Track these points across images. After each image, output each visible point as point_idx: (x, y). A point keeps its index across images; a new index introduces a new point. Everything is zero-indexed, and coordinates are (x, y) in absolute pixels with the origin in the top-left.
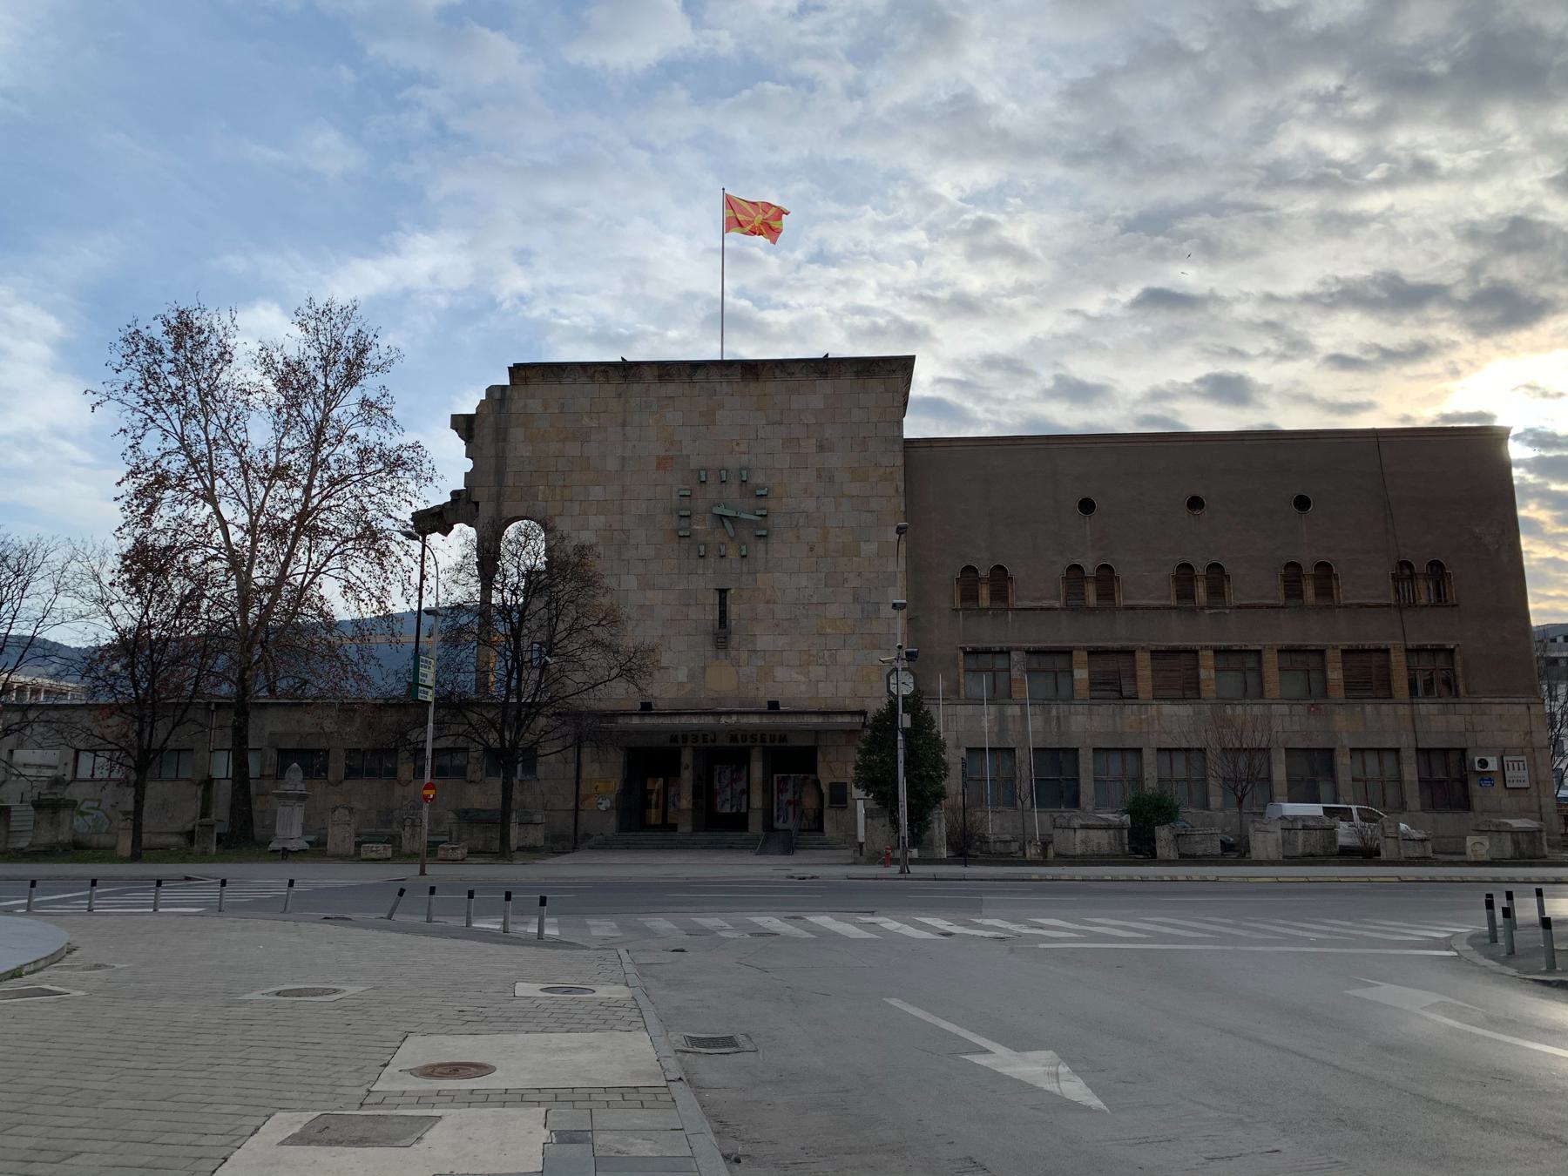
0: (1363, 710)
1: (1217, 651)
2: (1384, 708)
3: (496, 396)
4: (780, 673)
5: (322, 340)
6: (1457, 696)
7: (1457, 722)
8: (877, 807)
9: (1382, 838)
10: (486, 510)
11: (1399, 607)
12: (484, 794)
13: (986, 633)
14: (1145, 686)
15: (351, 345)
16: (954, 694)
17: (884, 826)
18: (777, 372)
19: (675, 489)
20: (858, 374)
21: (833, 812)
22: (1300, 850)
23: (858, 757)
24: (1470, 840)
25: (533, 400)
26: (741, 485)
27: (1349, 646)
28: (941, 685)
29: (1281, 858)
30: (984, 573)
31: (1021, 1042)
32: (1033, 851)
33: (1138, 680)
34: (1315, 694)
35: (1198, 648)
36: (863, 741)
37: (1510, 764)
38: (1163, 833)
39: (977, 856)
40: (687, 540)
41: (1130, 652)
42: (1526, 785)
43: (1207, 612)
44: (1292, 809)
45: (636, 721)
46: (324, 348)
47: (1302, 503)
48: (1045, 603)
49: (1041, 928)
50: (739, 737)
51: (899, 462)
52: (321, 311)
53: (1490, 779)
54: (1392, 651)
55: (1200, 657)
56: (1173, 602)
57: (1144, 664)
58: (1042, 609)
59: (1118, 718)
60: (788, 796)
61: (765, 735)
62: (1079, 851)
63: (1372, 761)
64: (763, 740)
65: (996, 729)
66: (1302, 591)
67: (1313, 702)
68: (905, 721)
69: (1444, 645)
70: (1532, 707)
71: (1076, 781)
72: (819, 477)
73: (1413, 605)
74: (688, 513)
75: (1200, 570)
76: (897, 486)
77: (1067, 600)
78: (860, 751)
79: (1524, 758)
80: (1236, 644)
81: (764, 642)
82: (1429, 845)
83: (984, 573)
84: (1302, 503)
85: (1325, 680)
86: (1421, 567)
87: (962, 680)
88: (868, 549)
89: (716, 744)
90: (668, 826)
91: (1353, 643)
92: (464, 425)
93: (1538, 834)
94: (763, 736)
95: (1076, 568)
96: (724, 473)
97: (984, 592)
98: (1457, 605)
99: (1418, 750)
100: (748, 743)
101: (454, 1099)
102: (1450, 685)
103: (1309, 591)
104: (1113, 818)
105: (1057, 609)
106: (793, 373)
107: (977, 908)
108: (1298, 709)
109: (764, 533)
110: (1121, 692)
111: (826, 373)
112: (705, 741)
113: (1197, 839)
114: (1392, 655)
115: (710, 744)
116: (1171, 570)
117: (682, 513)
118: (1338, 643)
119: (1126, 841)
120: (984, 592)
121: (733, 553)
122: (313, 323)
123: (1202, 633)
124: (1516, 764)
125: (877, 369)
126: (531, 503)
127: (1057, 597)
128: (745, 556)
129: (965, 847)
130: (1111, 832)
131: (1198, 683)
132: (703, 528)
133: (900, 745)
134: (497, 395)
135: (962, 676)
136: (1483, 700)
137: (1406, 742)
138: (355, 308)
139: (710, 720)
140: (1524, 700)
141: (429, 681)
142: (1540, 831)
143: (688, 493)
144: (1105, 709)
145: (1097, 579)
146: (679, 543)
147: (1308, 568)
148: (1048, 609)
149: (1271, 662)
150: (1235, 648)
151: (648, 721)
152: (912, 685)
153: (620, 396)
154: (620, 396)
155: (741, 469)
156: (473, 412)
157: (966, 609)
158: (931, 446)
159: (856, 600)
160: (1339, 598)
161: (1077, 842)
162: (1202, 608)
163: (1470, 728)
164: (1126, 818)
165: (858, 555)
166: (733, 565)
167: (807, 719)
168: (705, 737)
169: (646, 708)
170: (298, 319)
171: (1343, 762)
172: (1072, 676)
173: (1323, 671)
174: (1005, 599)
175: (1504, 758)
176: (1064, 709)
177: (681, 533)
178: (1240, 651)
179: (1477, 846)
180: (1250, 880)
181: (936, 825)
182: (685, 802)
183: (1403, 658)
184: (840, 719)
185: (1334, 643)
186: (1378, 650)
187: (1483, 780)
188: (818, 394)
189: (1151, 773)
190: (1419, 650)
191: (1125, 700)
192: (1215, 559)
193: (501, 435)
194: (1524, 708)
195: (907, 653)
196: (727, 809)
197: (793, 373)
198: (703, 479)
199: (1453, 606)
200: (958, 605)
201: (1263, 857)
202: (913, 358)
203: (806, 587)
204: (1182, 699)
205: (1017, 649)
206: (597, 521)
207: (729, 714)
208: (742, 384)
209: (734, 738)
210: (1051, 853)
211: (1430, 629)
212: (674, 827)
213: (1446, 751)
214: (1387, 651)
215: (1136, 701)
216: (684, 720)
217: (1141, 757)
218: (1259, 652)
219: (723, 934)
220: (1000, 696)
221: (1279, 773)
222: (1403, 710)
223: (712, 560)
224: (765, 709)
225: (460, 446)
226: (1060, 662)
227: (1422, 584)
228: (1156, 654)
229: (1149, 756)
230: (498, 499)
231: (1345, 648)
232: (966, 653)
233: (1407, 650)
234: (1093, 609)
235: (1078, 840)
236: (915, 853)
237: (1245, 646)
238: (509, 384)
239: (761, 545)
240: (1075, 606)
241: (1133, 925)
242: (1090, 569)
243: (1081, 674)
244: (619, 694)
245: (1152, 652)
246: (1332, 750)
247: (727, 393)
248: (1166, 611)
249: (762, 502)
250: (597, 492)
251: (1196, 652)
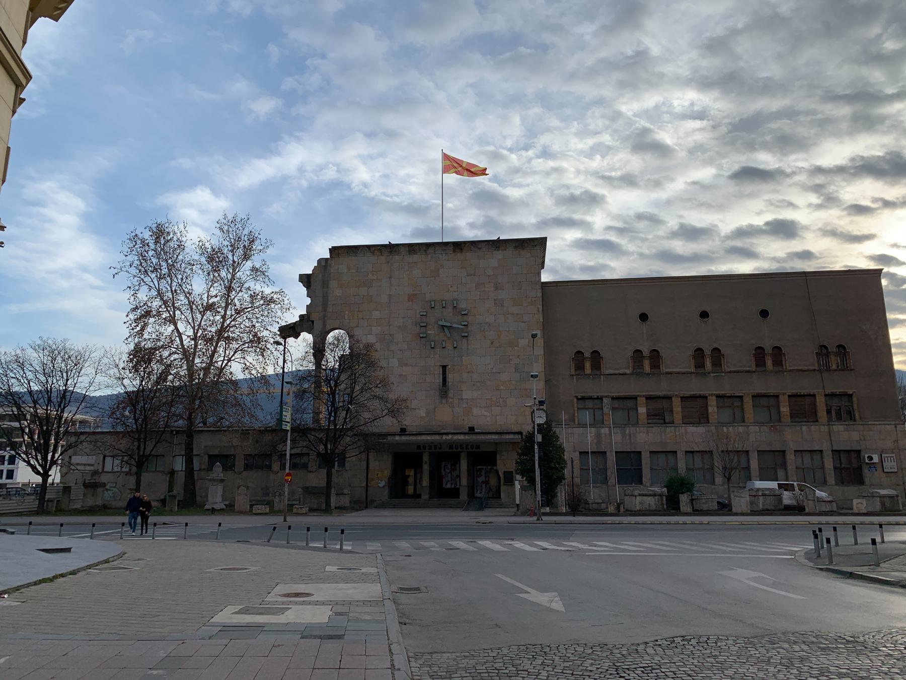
0: (801, 429)
1: (718, 397)
2: (814, 428)
3: (323, 264)
4: (476, 411)
5: (231, 237)
6: (855, 420)
7: (855, 435)
8: (528, 485)
9: (806, 501)
10: (318, 325)
11: (820, 371)
12: (317, 478)
13: (589, 388)
14: (678, 417)
15: (246, 239)
16: (572, 421)
17: (531, 495)
18: (472, 247)
19: (418, 311)
20: (516, 247)
21: (505, 487)
22: (761, 507)
23: (516, 457)
24: (855, 501)
25: (343, 265)
26: (453, 309)
28: (564, 417)
29: (749, 512)
30: (587, 355)
31: (543, 589)
32: (612, 508)
33: (674, 412)
34: (774, 420)
35: (707, 395)
36: (520, 448)
37: (886, 459)
38: (684, 498)
39: (582, 511)
40: (425, 339)
41: (669, 398)
42: (896, 470)
43: (712, 375)
44: (759, 484)
45: (397, 438)
46: (232, 240)
47: (764, 314)
48: (621, 371)
49: (595, 546)
50: (454, 446)
51: (540, 295)
52: (230, 221)
53: (875, 467)
54: (817, 396)
56: (693, 370)
57: (677, 404)
58: (620, 374)
59: (663, 434)
60: (481, 479)
61: (468, 445)
62: (638, 508)
63: (807, 458)
64: (467, 448)
65: (595, 441)
66: (765, 363)
67: (772, 424)
68: (539, 438)
69: (847, 392)
70: (898, 426)
71: (640, 470)
73: (828, 369)
74: (425, 324)
75: (707, 352)
77: (634, 368)
78: (518, 454)
79: (894, 455)
80: (728, 392)
81: (467, 395)
82: (834, 504)
83: (587, 355)
84: (764, 314)
85: (779, 412)
86: (832, 348)
87: (576, 414)
89: (441, 450)
90: (416, 496)
91: (795, 391)
92: (306, 280)
93: (896, 498)
94: (467, 446)
95: (638, 352)
96: (444, 302)
97: (588, 365)
98: (854, 370)
99: (832, 451)
100: (459, 450)
101: (296, 603)
102: (851, 416)
103: (769, 363)
104: (657, 489)
105: (628, 374)
106: (481, 248)
107: (568, 537)
108: (764, 428)
109: (466, 334)
110: (664, 420)
111: (499, 247)
112: (435, 449)
113: (704, 501)
114: (817, 398)
115: (438, 450)
116: (691, 352)
117: (422, 325)
119: (665, 502)
120: (588, 365)
121: (449, 346)
122: (226, 228)
123: (708, 386)
124: (889, 458)
125: (526, 245)
126: (341, 321)
127: (628, 368)
128: (455, 348)
129: (577, 506)
130: (656, 498)
131: (708, 415)
133: (536, 451)
134: (323, 264)
135: (576, 411)
136: (870, 423)
137: (826, 446)
138: (248, 219)
139: (437, 437)
140: (893, 423)
141: (288, 419)
142: (897, 496)
143: (425, 314)
144: (656, 430)
145: (650, 358)
146: (421, 341)
147: (768, 350)
148: (623, 374)
149: (748, 403)
150: (728, 395)
151: (404, 438)
152: (545, 418)
153: (388, 262)
154: (388, 262)
155: (454, 300)
156: (311, 273)
157: (578, 375)
159: (517, 370)
160: (786, 366)
161: (637, 503)
162: (709, 373)
163: (863, 439)
164: (665, 490)
167: (489, 437)
168: (435, 446)
169: (403, 431)
170: (218, 226)
171: (790, 458)
172: (637, 410)
173: (778, 407)
174: (599, 368)
175: (883, 455)
176: (633, 429)
177: (421, 336)
178: (731, 397)
179: (859, 504)
180: (727, 523)
181: (559, 494)
182: (426, 482)
183: (823, 399)
184: (507, 437)
186: (809, 395)
187: (870, 467)
188: (495, 259)
189: (682, 465)
190: (833, 395)
191: (668, 425)
192: (716, 346)
193: (325, 284)
194: (894, 426)
195: (539, 402)
196: (449, 486)
197: (481, 248)
198: (433, 306)
199: (851, 370)
201: (739, 511)
202: (546, 238)
203: (489, 364)
204: (698, 423)
205: (606, 397)
206: (376, 330)
207: (447, 434)
208: (453, 254)
209: (451, 447)
210: (622, 509)
211: (838, 383)
212: (419, 496)
213: (848, 452)
214: (814, 396)
215: (672, 425)
216: (423, 437)
217: (676, 456)
218: (741, 397)
219: (432, 549)
220: (597, 423)
221: (754, 464)
222: (824, 429)
224: (467, 431)
225: (304, 290)
226: (630, 403)
227: (833, 357)
228: (683, 398)
229: (681, 456)
230: (324, 319)
231: (790, 394)
232: (578, 399)
233: (826, 395)
234: (648, 374)
235: (637, 502)
236: (548, 509)
238: (329, 257)
239: (464, 341)
240: (638, 372)
241: (642, 544)
242: (646, 352)
243: (642, 410)
244: (388, 424)
245: (682, 398)
246: (784, 452)
247: (445, 260)
248: (689, 375)
249: (465, 318)
250: (376, 314)
251: (706, 397)
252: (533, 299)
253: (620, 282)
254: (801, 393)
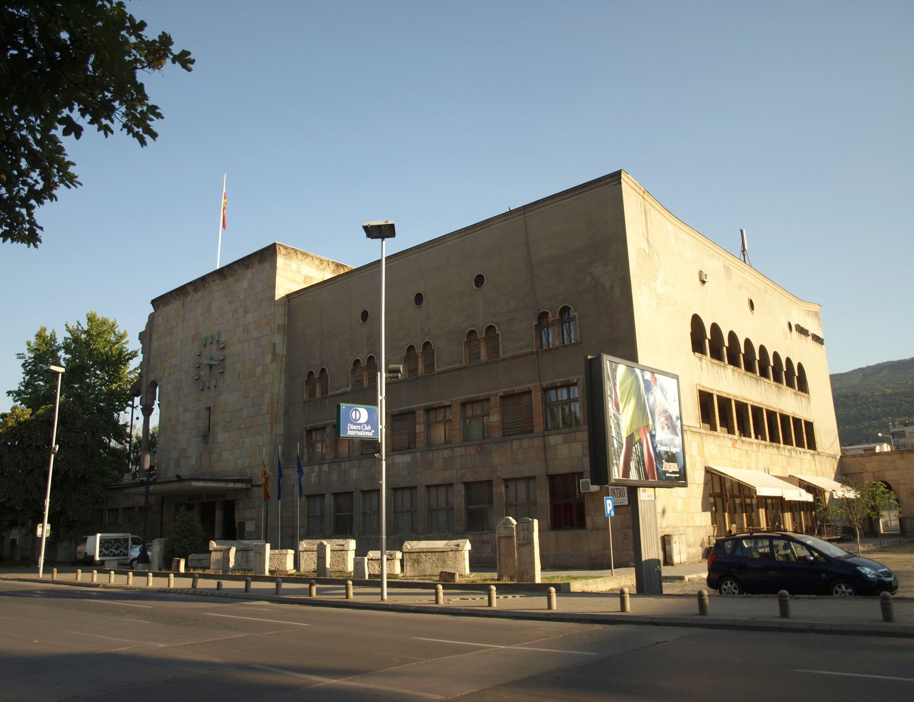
2: (526, 443)
20: (260, 261)
27: (504, 392)
55: (417, 417)
72: (244, 330)
88: (259, 370)
114: (533, 395)
118: (497, 391)
150: (435, 406)
158: (299, 296)
165: (255, 376)
185: (495, 392)
193: (150, 341)
200: (306, 397)
214: (529, 392)
237: (441, 403)
238: (154, 311)
242: (364, 363)
252: (269, 317)
253: (347, 276)
254: (513, 391)
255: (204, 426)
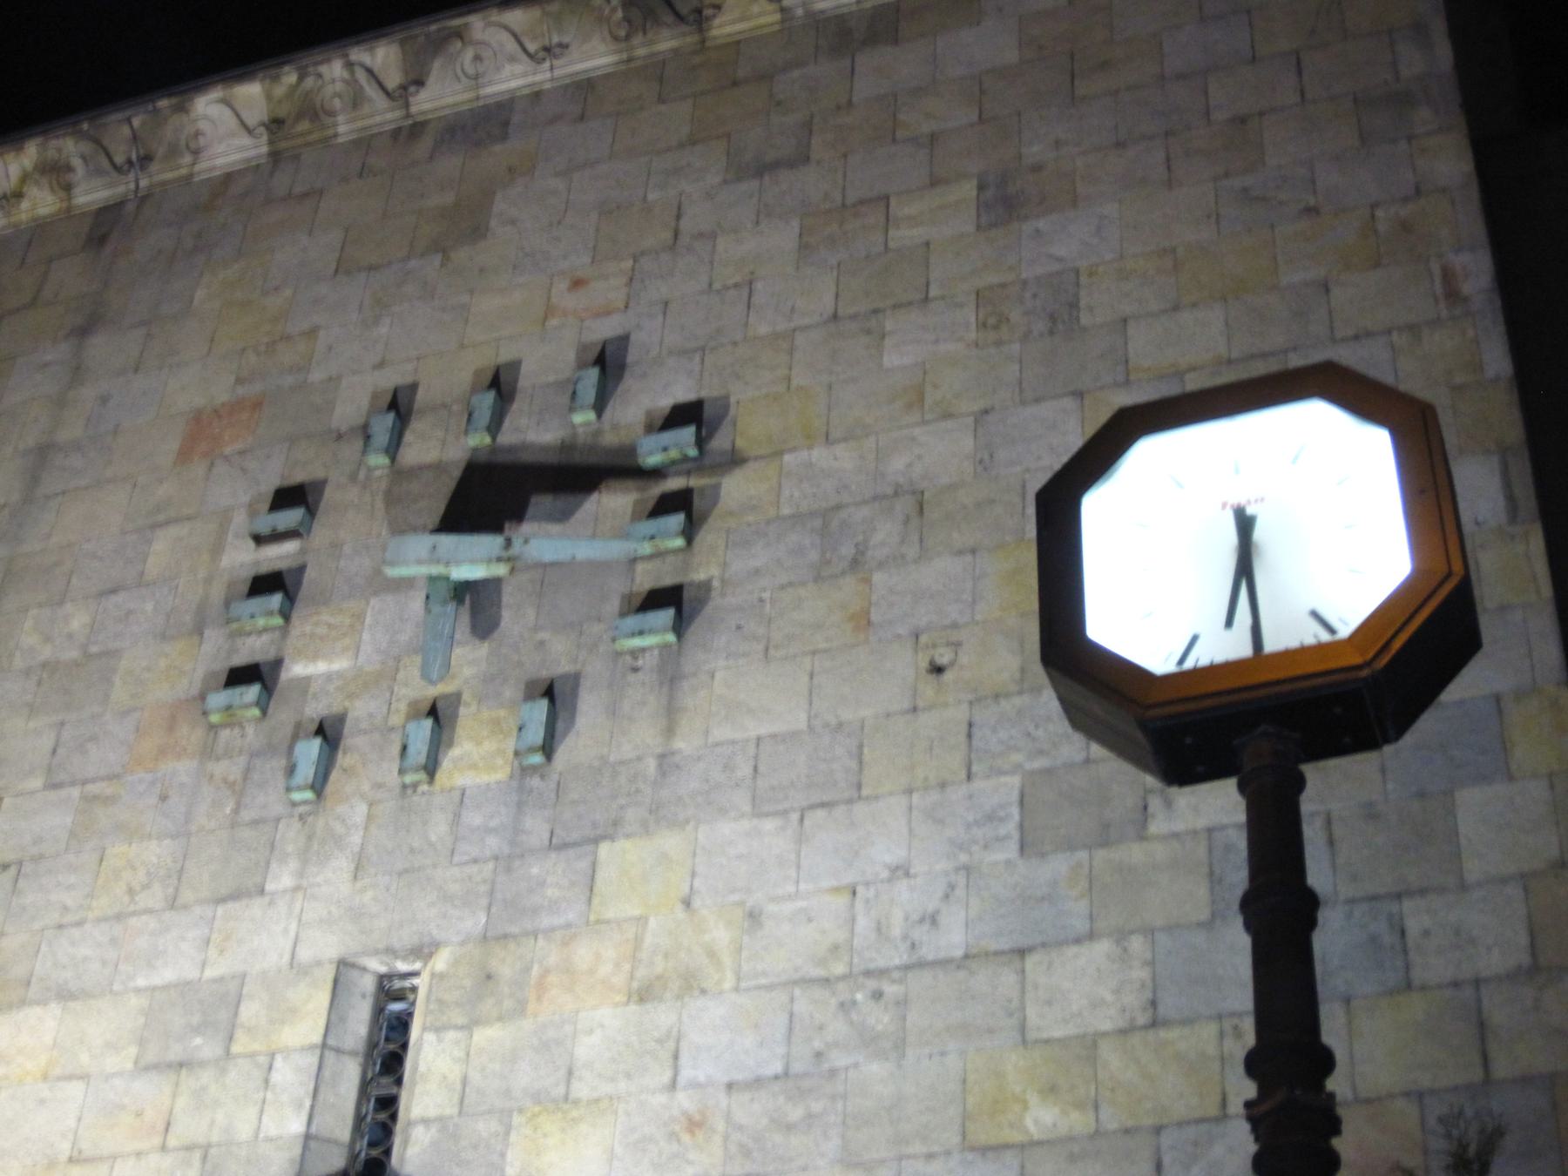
76: (1448, 275)
132: (340, 664)
166: (473, 818)
203: (901, 871)
223: (361, 809)
255: (296, 1126)
